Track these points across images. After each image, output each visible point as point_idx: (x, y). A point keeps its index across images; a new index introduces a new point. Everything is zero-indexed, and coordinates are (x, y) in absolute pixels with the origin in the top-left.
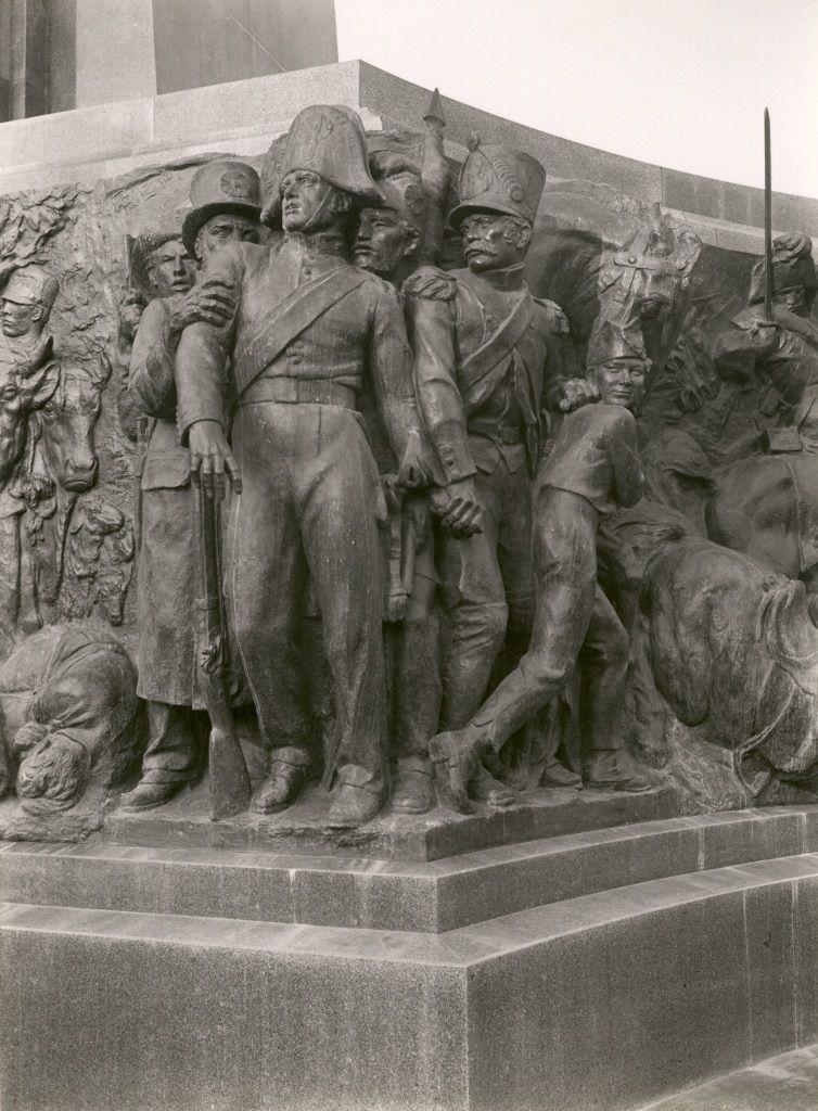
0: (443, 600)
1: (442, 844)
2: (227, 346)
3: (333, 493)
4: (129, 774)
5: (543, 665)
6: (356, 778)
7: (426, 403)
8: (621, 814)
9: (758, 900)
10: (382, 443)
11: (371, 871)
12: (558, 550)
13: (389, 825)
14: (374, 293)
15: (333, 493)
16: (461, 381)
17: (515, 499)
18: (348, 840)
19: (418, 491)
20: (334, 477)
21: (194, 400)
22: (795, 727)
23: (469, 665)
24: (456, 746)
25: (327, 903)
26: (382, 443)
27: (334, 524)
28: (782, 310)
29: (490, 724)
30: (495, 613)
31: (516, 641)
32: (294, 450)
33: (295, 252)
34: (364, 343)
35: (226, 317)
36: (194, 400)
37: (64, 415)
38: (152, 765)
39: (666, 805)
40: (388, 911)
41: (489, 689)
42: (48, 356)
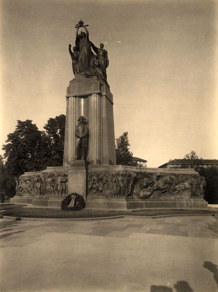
0: (125, 190)
1: (126, 199)
2: (118, 180)
3: (122, 186)
4: (112, 197)
5: (129, 192)
6: (123, 196)
7: (125, 182)
8: (132, 199)
9: (138, 202)
10: (123, 183)
11: (123, 200)
12: (130, 188)
13: (124, 198)
14: (124, 178)
15: (122, 186)
16: (126, 181)
17: (128, 186)
18: (122, 199)
19: (125, 186)
20: (122, 185)
21: (117, 182)
22: (140, 195)
23: (126, 192)
24: (126, 195)
25: (121, 201)
26: (123, 183)
27: (122, 187)
28: (141, 175)
29: (127, 195)
30: (127, 190)
31: (128, 192)
32: (120, 184)
33: (120, 176)
34: (123, 180)
35: (118, 179)
36: (117, 182)
37: (109, 181)
38: (113, 196)
39: (134, 199)
40: (124, 201)
41: (127, 193)
42: (108, 179)
